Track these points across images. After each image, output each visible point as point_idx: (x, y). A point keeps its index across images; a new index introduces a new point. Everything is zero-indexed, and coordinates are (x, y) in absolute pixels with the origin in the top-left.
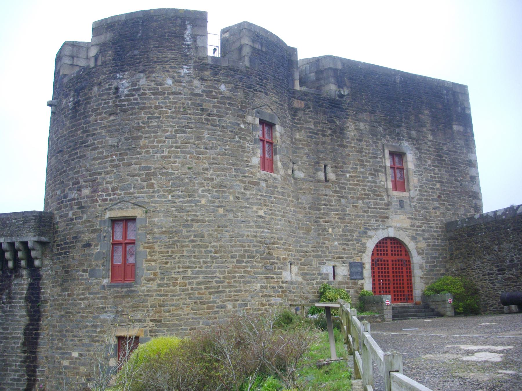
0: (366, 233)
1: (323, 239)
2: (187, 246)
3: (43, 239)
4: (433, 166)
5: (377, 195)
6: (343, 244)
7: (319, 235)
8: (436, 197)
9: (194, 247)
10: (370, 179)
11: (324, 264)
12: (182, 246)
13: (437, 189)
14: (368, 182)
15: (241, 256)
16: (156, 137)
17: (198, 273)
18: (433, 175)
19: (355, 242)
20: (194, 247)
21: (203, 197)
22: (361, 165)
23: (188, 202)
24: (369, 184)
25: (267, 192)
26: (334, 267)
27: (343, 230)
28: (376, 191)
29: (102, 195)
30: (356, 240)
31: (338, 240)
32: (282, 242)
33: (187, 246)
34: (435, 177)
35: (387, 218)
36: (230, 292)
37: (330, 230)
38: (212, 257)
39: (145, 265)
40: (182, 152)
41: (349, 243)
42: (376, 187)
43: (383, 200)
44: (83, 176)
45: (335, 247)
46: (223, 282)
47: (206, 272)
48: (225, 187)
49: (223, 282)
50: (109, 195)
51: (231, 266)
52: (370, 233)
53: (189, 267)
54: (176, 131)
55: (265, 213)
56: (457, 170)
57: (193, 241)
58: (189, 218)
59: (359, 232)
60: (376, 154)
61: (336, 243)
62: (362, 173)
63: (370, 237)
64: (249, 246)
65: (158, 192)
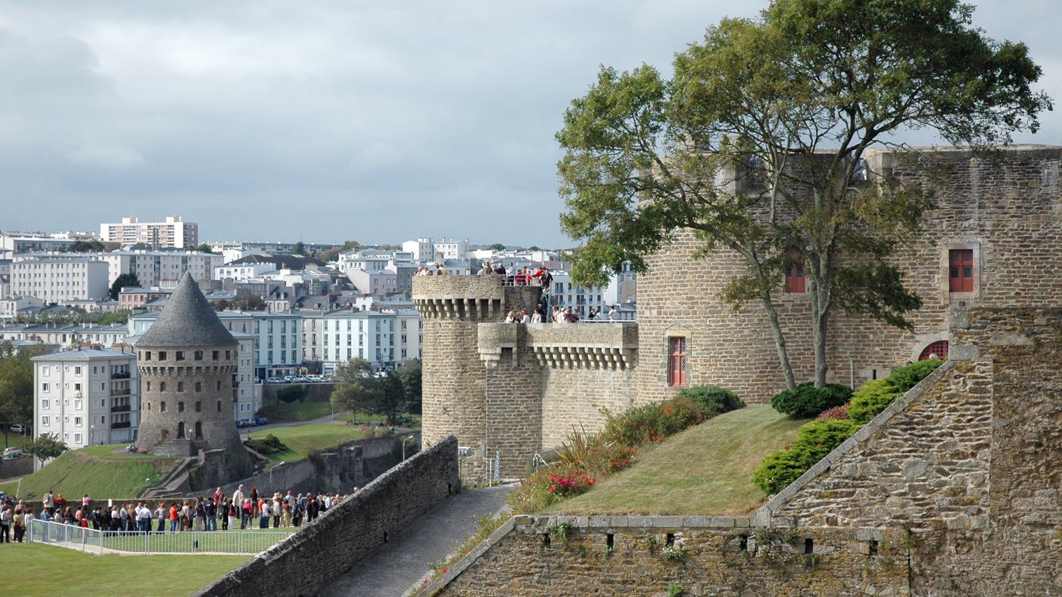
0: (913, 337)
1: (864, 345)
2: (720, 361)
3: (631, 346)
4: (1013, 259)
5: (931, 299)
6: (885, 349)
7: (859, 341)
8: (1012, 294)
9: (725, 361)
10: (922, 281)
11: (864, 368)
12: (716, 361)
13: (1017, 285)
14: (919, 285)
15: (763, 367)
16: (697, 273)
17: (730, 381)
18: (1012, 270)
19: (899, 347)
20: (725, 361)
21: (732, 321)
22: (912, 268)
23: (721, 326)
24: (921, 288)
25: (792, 311)
26: (875, 371)
27: (886, 337)
28: (928, 294)
29: (663, 318)
30: (901, 345)
31: (880, 345)
32: (810, 352)
33: (720, 361)
34: (1014, 272)
35: (942, 321)
36: (754, 396)
37: (871, 336)
38: (739, 369)
39: (691, 375)
40: (716, 285)
41: (892, 348)
42: (929, 290)
43: (939, 303)
44: (652, 300)
45: (878, 353)
46: (747, 388)
47: (733, 381)
48: (750, 312)
49: (747, 388)
50: (668, 318)
51: (754, 376)
52: (917, 337)
53: (720, 377)
54: (712, 268)
55: (790, 330)
56: (1050, 260)
57: (724, 357)
58: (722, 339)
59: (905, 337)
60: (933, 255)
61: (877, 349)
62: (912, 277)
63: (918, 341)
64: (771, 359)
65: (700, 317)
